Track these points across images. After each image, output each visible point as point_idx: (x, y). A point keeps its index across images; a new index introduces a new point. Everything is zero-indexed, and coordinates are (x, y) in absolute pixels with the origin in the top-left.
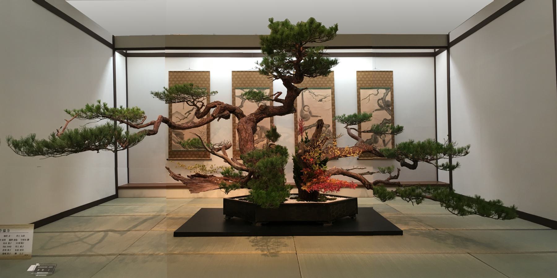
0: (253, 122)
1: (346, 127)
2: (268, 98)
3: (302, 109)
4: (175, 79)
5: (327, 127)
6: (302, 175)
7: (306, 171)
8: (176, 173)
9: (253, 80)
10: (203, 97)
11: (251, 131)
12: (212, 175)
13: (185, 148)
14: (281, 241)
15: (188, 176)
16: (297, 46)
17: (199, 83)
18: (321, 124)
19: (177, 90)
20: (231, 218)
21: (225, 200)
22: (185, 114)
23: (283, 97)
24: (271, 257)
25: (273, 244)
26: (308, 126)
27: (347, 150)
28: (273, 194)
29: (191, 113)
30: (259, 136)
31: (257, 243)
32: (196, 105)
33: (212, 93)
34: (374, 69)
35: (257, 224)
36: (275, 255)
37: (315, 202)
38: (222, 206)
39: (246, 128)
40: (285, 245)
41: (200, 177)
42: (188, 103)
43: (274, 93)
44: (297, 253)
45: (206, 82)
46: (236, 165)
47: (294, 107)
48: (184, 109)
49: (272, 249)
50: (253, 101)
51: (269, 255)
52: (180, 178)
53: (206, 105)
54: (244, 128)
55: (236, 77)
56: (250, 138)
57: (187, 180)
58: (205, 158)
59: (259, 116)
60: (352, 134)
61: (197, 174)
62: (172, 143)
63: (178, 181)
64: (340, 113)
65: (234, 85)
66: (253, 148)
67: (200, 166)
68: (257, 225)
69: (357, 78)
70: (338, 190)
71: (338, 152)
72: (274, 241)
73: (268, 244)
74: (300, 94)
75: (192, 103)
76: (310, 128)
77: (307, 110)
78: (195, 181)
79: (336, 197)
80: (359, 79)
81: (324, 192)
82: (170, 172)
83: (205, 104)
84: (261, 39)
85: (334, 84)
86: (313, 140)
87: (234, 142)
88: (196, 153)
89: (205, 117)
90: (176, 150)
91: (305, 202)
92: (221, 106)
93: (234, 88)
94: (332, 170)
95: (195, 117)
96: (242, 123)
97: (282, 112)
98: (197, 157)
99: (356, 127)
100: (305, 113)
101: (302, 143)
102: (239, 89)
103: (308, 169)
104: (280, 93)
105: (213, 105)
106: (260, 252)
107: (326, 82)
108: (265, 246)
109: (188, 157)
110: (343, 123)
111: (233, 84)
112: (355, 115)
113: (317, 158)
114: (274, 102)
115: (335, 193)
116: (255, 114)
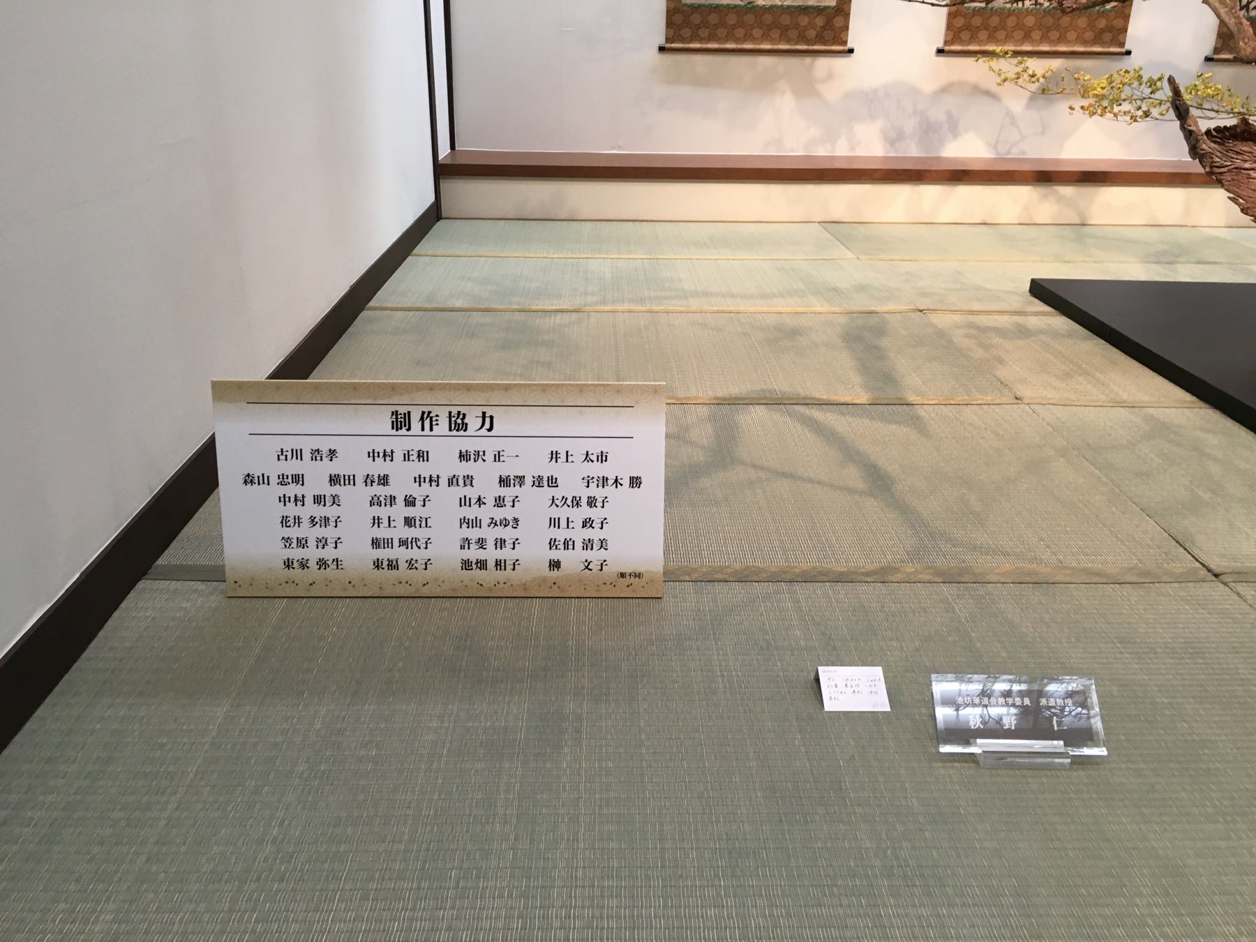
88: (785, 20)
98: (788, 41)
109: (748, 37)
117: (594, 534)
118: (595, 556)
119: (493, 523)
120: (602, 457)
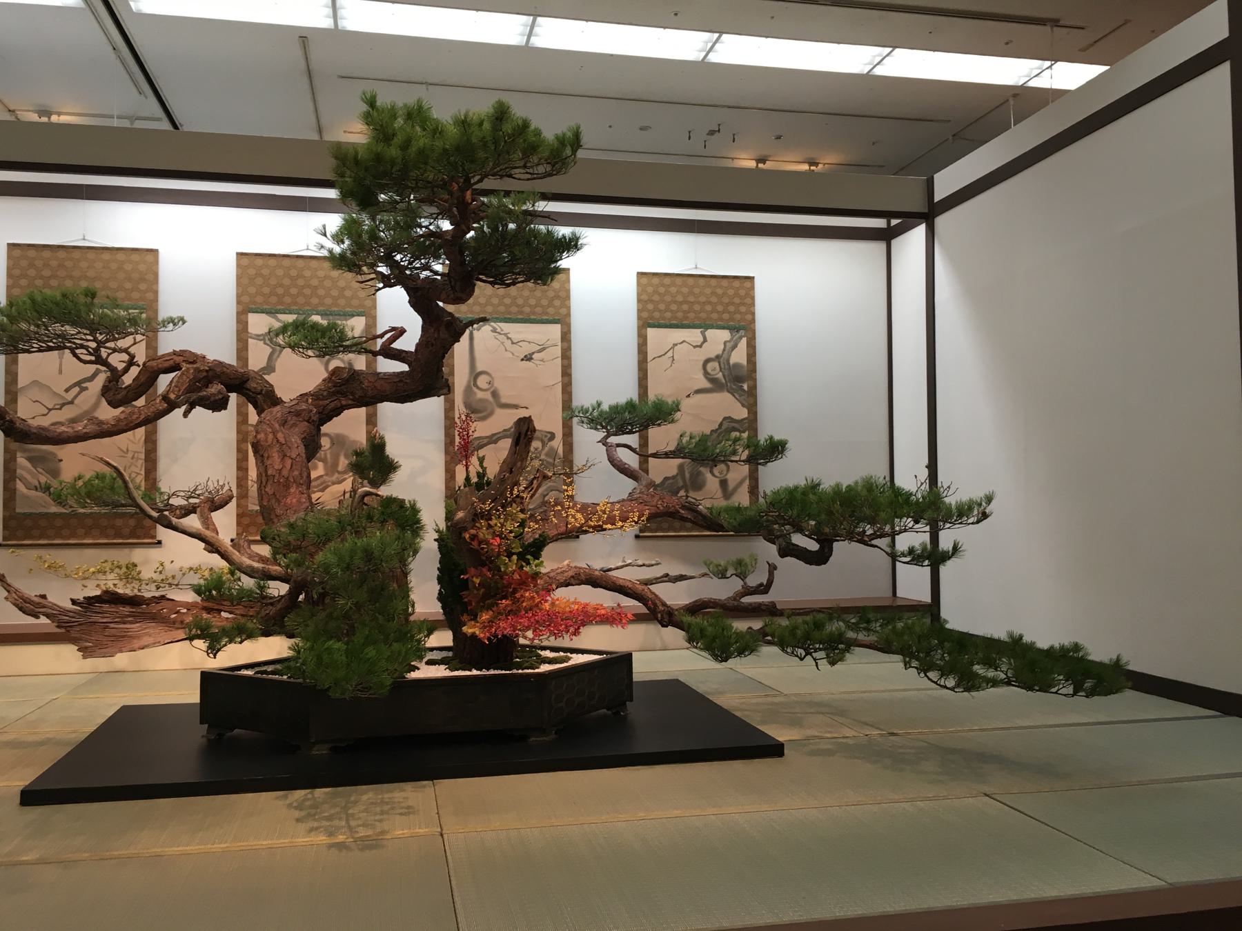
0: (308, 421)
1: (604, 442)
2: (359, 347)
3: (469, 382)
4: (32, 272)
6: (467, 588)
7: (477, 578)
8: (31, 589)
9: (309, 286)
10: (131, 337)
11: (302, 449)
12: (163, 597)
13: (63, 507)
14: (394, 798)
15: (72, 600)
16: (456, 187)
18: (527, 431)
19: (36, 311)
20: (229, 734)
21: (208, 679)
22: (67, 390)
23: (408, 343)
25: (366, 810)
26: (487, 437)
27: (604, 512)
28: (371, 652)
29: (86, 389)
30: (329, 464)
31: (313, 811)
32: (105, 363)
33: (163, 321)
37: (504, 672)
38: (193, 696)
40: (406, 811)
42: (75, 355)
43: (379, 332)
44: (444, 832)
45: (143, 286)
46: (247, 561)
47: (445, 377)
48: (60, 372)
49: (363, 825)
50: (310, 353)
53: (144, 364)
54: (278, 441)
55: (252, 272)
56: (296, 473)
57: (71, 614)
58: (138, 538)
59: (327, 402)
60: (621, 460)
61: (106, 592)
62: (15, 489)
63: (38, 617)
64: (584, 397)
65: (242, 298)
66: (307, 504)
67: (120, 567)
69: (639, 295)
70: (576, 633)
71: (579, 516)
72: (368, 799)
73: (350, 811)
74: (465, 338)
75: (91, 354)
76: (495, 442)
79: (569, 654)
80: (645, 297)
81: (532, 640)
82: (8, 588)
83: (141, 358)
84: (336, 158)
85: (569, 308)
87: (241, 486)
88: (104, 522)
89: (141, 402)
90: (31, 514)
91: (475, 672)
94: (559, 571)
95: (104, 400)
96: (271, 426)
98: (107, 537)
99: (632, 440)
100: (480, 395)
101: (467, 489)
102: (263, 312)
103: (484, 570)
104: (399, 332)
105: (167, 365)
106: (324, 838)
107: (544, 302)
108: (340, 819)
110: (596, 429)
111: (239, 296)
112: (630, 406)
113: (513, 534)
114: (380, 358)
115: (566, 642)
116: (316, 395)
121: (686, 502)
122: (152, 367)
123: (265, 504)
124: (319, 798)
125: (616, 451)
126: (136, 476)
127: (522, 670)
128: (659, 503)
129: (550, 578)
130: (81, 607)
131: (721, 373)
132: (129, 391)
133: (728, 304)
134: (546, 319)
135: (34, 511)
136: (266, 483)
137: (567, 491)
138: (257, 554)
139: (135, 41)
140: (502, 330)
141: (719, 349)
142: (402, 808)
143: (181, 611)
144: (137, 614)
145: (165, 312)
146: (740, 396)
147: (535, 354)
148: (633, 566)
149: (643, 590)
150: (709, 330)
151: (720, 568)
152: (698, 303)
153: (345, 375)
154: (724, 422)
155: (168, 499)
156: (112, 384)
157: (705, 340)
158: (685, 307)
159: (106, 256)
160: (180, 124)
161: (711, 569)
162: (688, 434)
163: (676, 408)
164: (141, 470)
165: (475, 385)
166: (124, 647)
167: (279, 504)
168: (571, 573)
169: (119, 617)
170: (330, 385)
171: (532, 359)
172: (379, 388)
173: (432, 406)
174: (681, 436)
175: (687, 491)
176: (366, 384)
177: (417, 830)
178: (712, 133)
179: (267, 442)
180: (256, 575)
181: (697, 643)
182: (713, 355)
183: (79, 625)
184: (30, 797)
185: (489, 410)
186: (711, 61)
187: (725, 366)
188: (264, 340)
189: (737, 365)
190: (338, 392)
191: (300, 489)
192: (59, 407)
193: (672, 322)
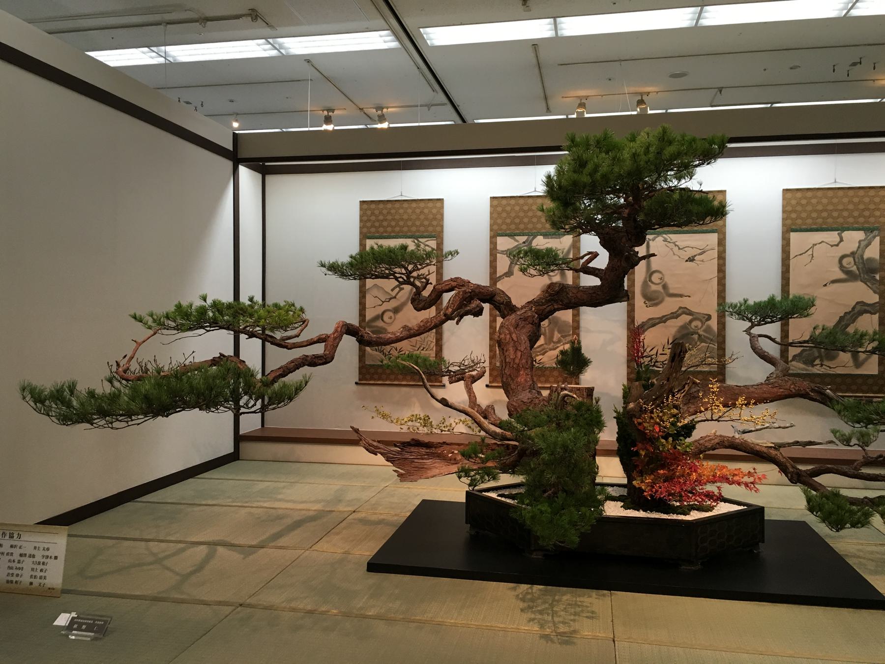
0: (532, 324)
1: (748, 331)
3: (646, 278)
4: (373, 218)
5: (704, 320)
7: (643, 450)
11: (528, 343)
14: (584, 602)
17: (422, 225)
18: (681, 352)
22: (392, 290)
24: (559, 646)
25: (565, 610)
26: (658, 318)
29: (403, 289)
30: (547, 337)
31: (531, 604)
33: (446, 254)
34: (825, 185)
35: (535, 554)
36: (567, 639)
38: (462, 499)
39: (515, 339)
41: (418, 446)
44: (615, 639)
45: (435, 223)
49: (564, 623)
51: (555, 639)
52: (379, 448)
54: (513, 340)
55: (500, 209)
56: (524, 361)
60: (762, 349)
64: (734, 297)
66: (531, 382)
67: (420, 419)
68: (534, 556)
69: (784, 206)
72: (567, 600)
76: (665, 322)
77: (658, 281)
78: (407, 456)
80: (789, 208)
83: (433, 279)
86: (662, 386)
87: (492, 350)
90: (374, 365)
92: (465, 291)
93: (494, 235)
94: (707, 439)
96: (508, 329)
97: (597, 300)
98: (414, 380)
99: (773, 329)
100: (654, 287)
104: (595, 255)
105: (447, 287)
106: (538, 629)
110: (744, 320)
111: (491, 226)
112: (771, 301)
117: (42, 574)
118: (43, 581)
119: (16, 568)
120: (48, 549)
121: (816, 387)
122: (439, 289)
123: (505, 380)
124: (536, 593)
125: (757, 341)
126: (431, 343)
127: (677, 514)
128: (792, 387)
129: (700, 444)
130: (400, 448)
131: (855, 267)
132: (425, 303)
133: (863, 210)
134: (706, 230)
135: (375, 364)
136: (505, 367)
137: (713, 388)
138: (499, 418)
139: (430, 62)
140: (671, 240)
141: (854, 247)
142: (588, 612)
143: (455, 452)
144: (430, 454)
145: (447, 248)
146: (872, 285)
147: (697, 256)
148: (770, 428)
149: (777, 455)
150: (845, 232)
151: (845, 437)
152: (836, 210)
153: (557, 289)
154: (857, 306)
155: (449, 366)
156: (416, 297)
157: (841, 240)
158: (825, 214)
159: (414, 205)
160: (458, 105)
161: (837, 436)
162: (821, 327)
163: (811, 303)
164: (433, 339)
165: (650, 280)
166: (423, 475)
167: (513, 382)
168: (717, 441)
169: (420, 456)
170: (547, 295)
171: (694, 260)
172: (579, 297)
173: (618, 310)
174: (814, 328)
175: (822, 360)
176: (571, 295)
177: (598, 634)
178: (854, 64)
179: (506, 340)
180: (498, 438)
181: (817, 513)
182: (848, 252)
183: (399, 459)
184: (374, 566)
185: (660, 299)
186: (853, 15)
187: (859, 259)
188: (506, 254)
189: (870, 260)
190: (552, 300)
191: (526, 372)
192: (388, 300)
193: (812, 227)
